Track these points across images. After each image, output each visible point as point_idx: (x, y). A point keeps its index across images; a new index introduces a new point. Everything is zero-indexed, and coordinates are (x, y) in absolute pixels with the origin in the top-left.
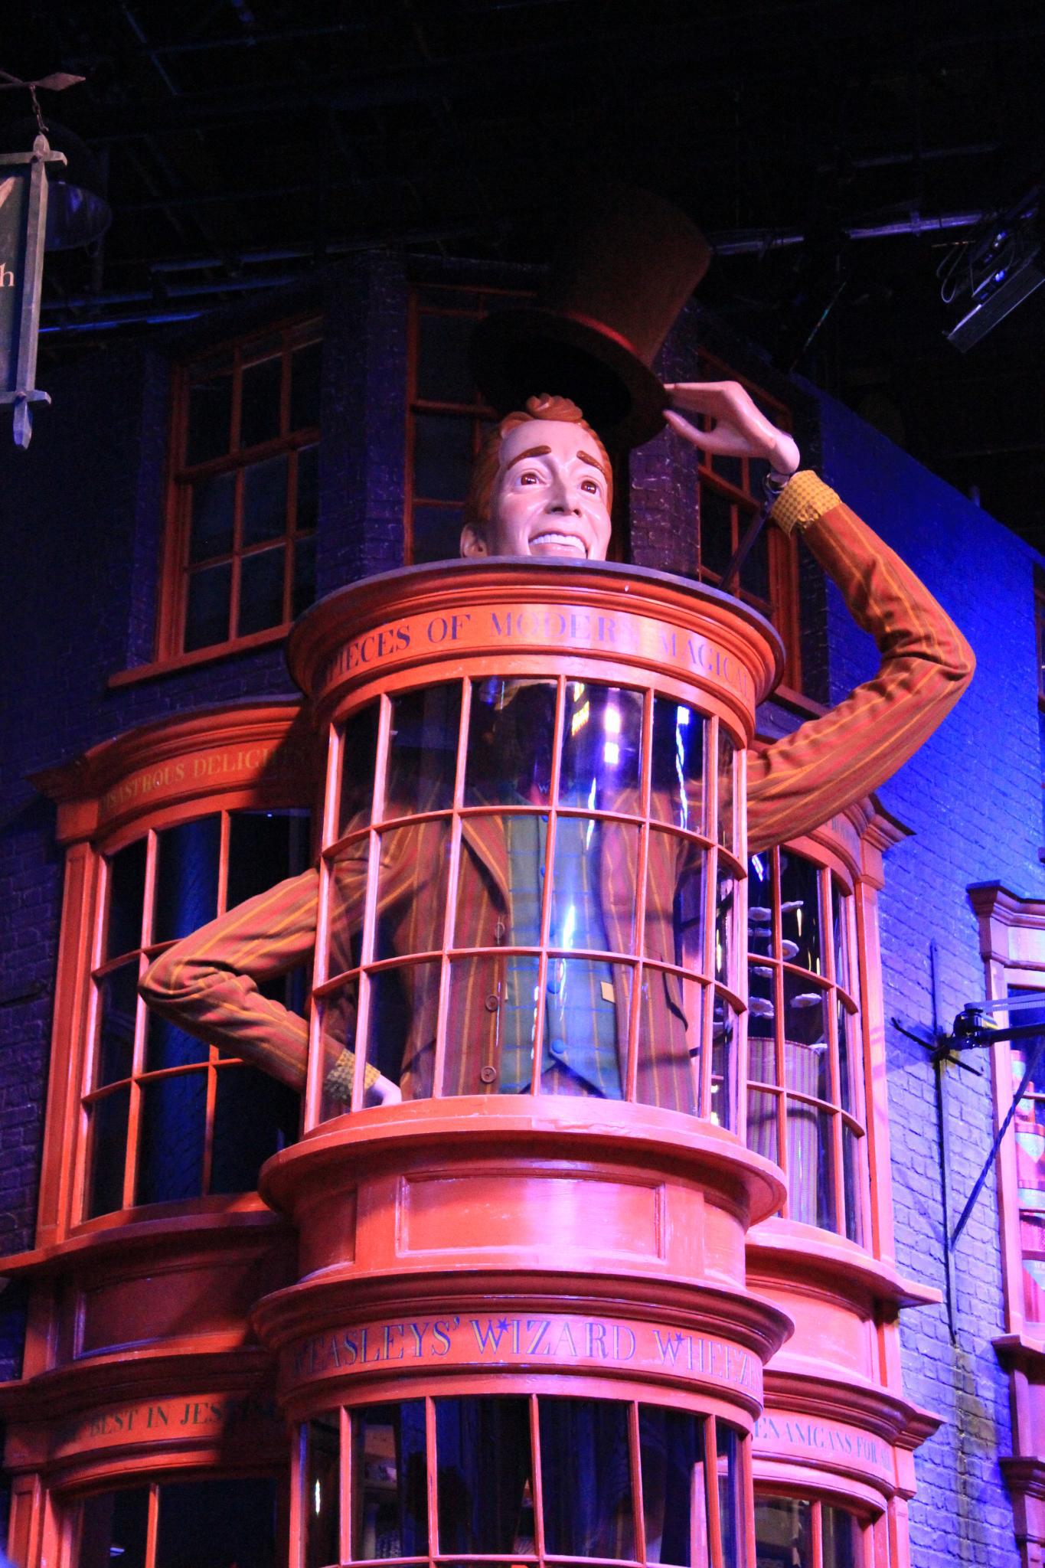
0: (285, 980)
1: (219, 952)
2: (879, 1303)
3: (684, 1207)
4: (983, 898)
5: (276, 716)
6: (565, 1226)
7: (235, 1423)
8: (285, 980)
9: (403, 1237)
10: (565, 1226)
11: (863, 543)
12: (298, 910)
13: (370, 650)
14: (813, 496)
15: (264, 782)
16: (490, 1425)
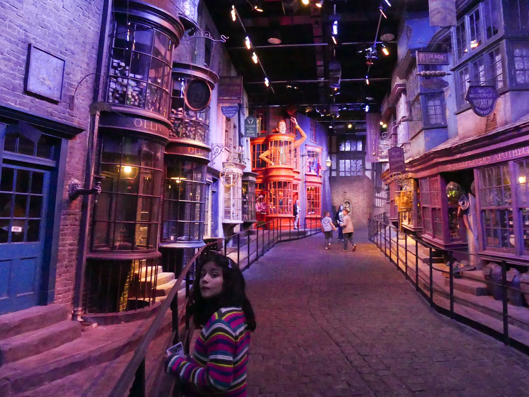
0: (267, 157)
1: (263, 156)
2: (299, 173)
3: (290, 171)
4: (306, 145)
5: (265, 138)
6: (283, 173)
7: (263, 180)
8: (267, 157)
9: (275, 173)
10: (283, 173)
11: (301, 130)
12: (267, 153)
13: (272, 138)
14: (298, 127)
15: (263, 142)
16: (280, 183)
